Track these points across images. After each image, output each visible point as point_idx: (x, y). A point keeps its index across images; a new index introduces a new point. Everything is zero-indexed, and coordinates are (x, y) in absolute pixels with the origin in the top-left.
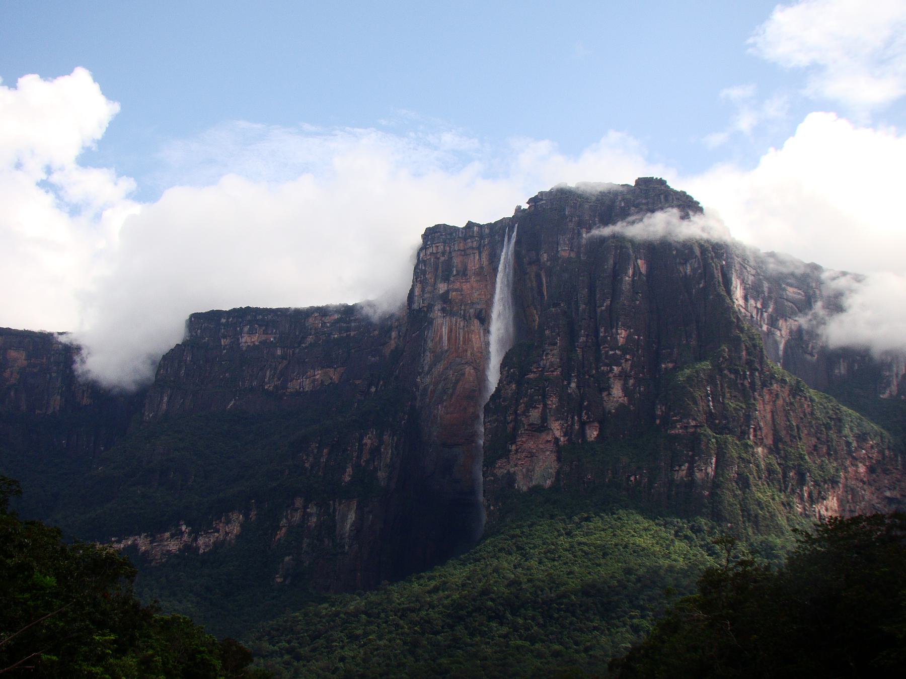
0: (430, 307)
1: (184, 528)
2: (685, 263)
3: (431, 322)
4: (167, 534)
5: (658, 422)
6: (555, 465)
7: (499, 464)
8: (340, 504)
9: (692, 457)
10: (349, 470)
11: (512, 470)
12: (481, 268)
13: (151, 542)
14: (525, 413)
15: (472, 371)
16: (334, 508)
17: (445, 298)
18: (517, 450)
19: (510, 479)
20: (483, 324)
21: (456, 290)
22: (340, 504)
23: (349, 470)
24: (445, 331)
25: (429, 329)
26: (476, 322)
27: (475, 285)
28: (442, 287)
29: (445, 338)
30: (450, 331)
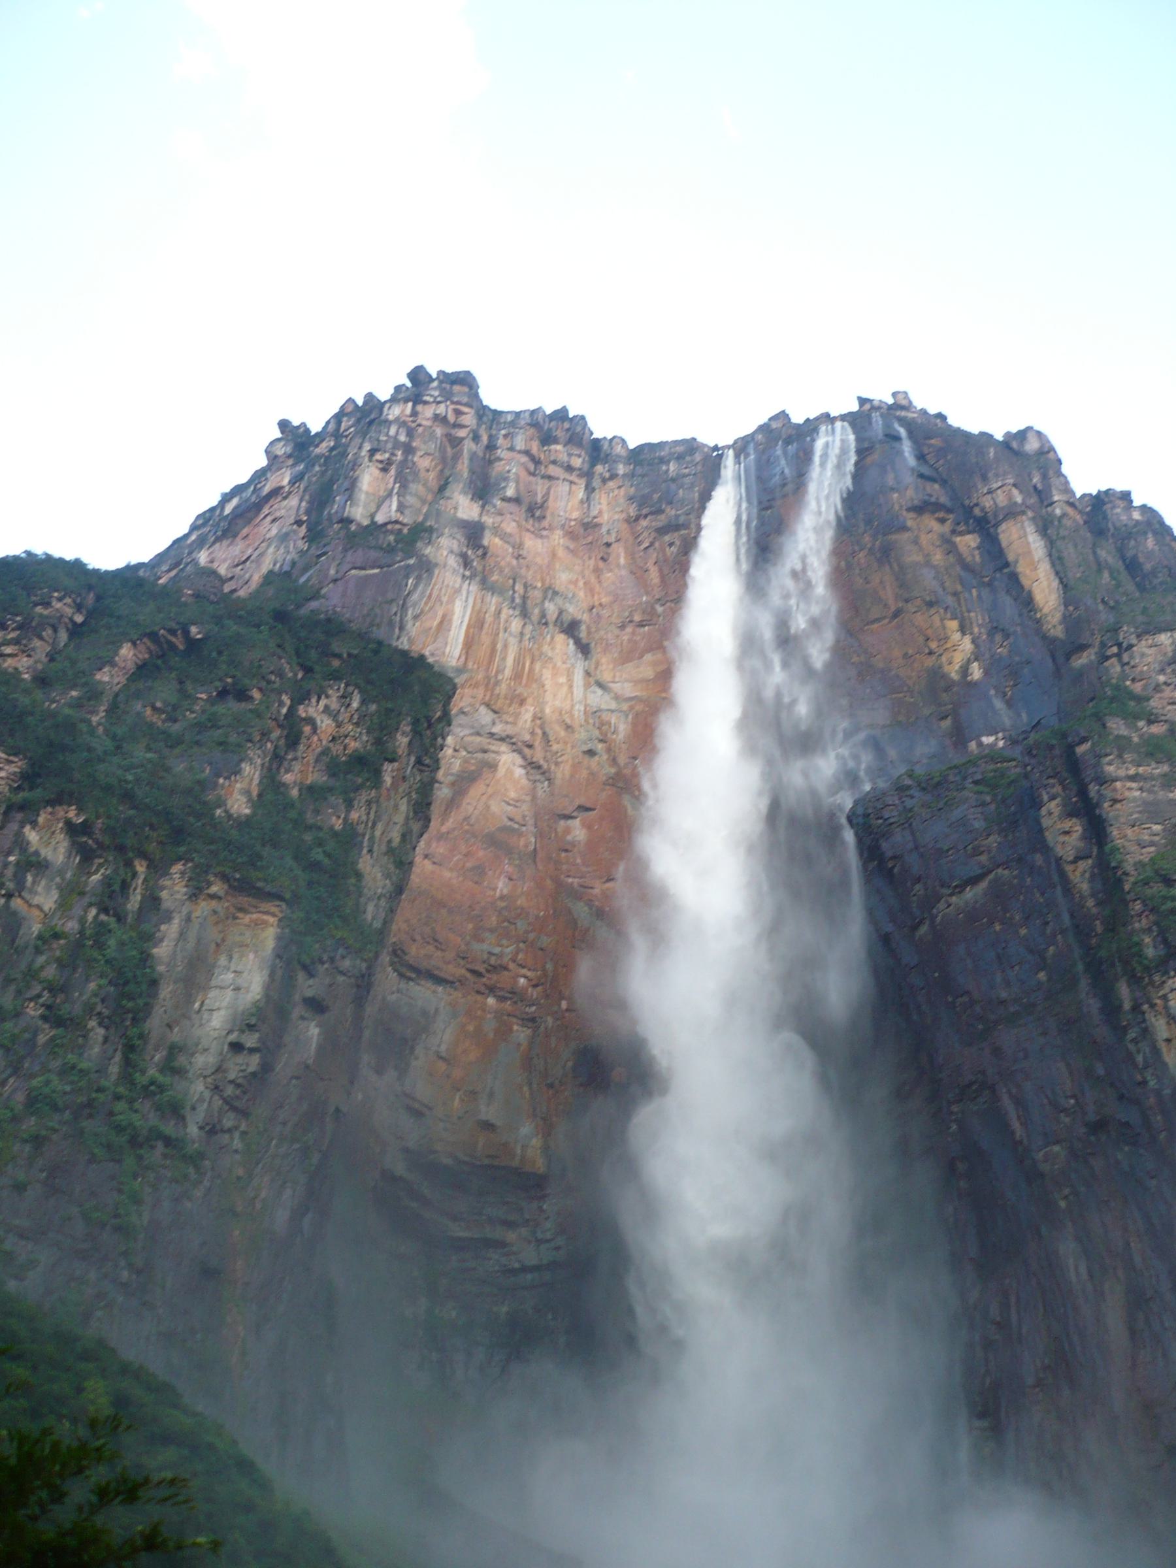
0: (421, 532)
3: (426, 568)
8: (194, 896)
10: (251, 773)
15: (519, 772)
16: (152, 901)
17: (473, 533)
20: (586, 659)
21: (505, 537)
22: (196, 893)
23: (251, 773)
24: (461, 614)
25: (419, 578)
27: (561, 553)
28: (466, 508)
30: (477, 623)
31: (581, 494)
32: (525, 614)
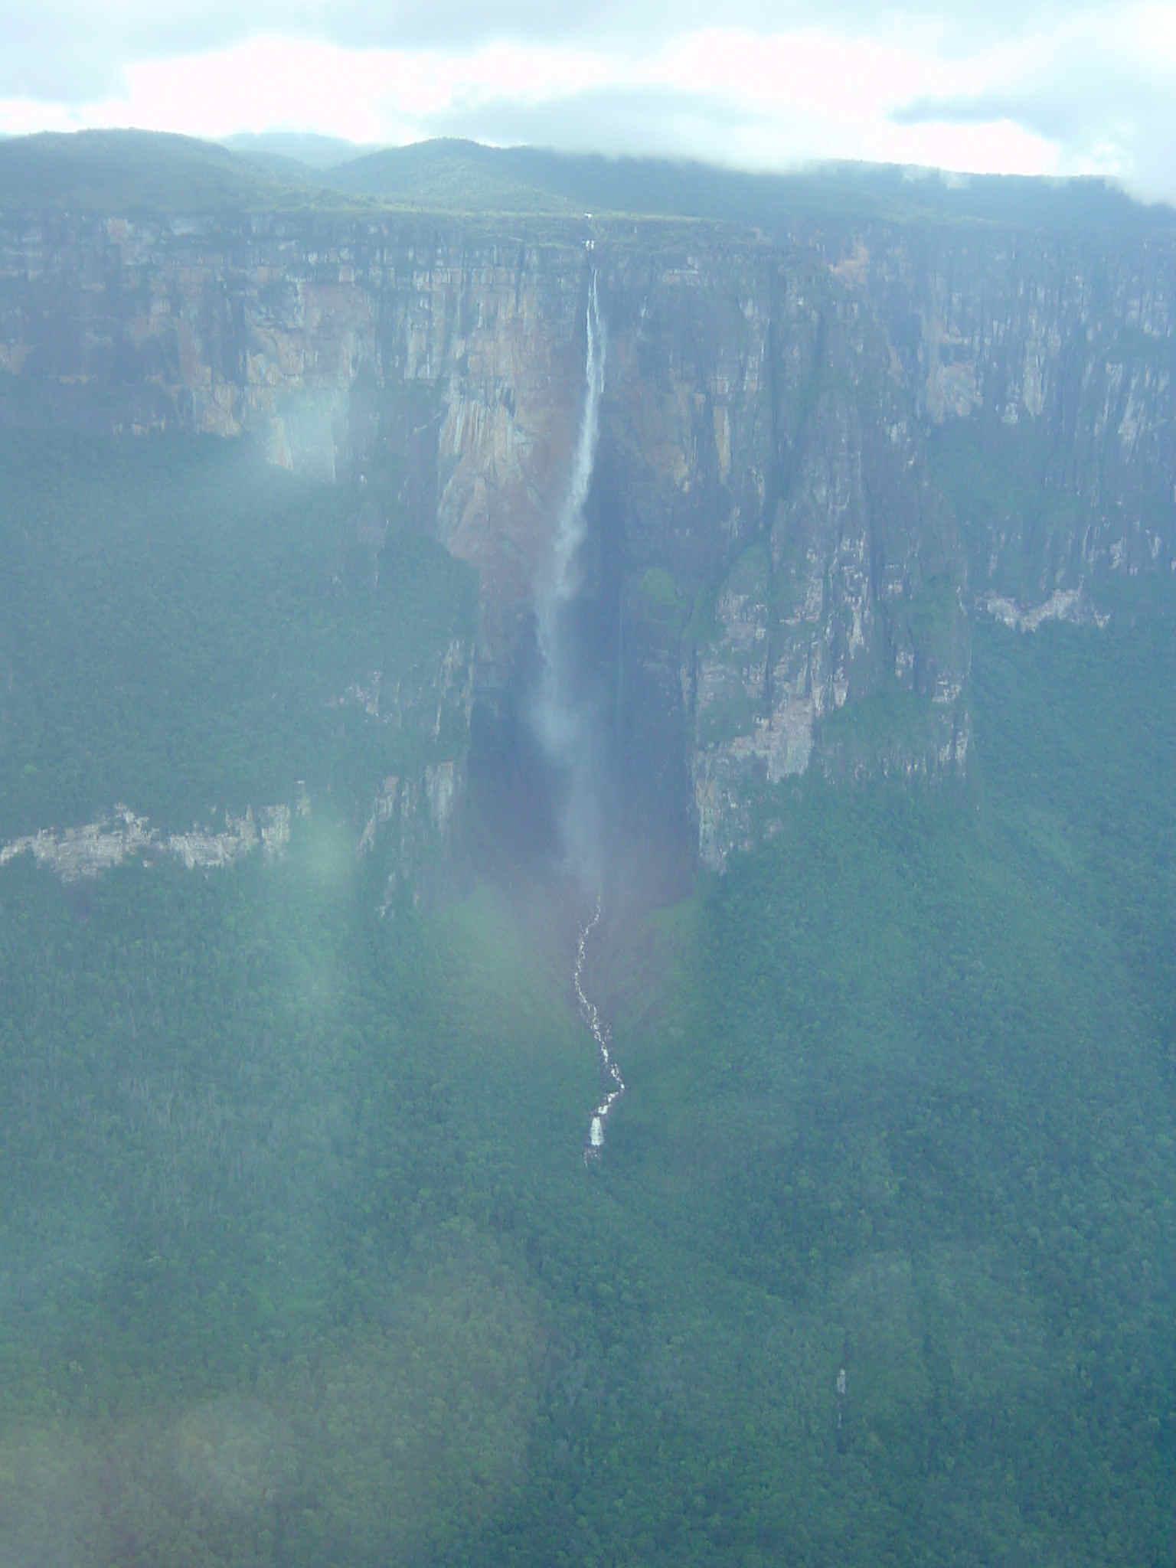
0: (441, 383)
1: (129, 817)
2: (892, 424)
3: (445, 409)
4: (92, 828)
5: (899, 673)
6: (810, 744)
7: (738, 740)
9: (956, 731)
11: (760, 753)
12: (517, 320)
13: (56, 843)
14: (789, 677)
17: (462, 366)
18: (770, 729)
19: (760, 767)
24: (460, 423)
26: (502, 412)
29: (458, 437)
30: (467, 423)
31: (513, 301)
32: (487, 404)
